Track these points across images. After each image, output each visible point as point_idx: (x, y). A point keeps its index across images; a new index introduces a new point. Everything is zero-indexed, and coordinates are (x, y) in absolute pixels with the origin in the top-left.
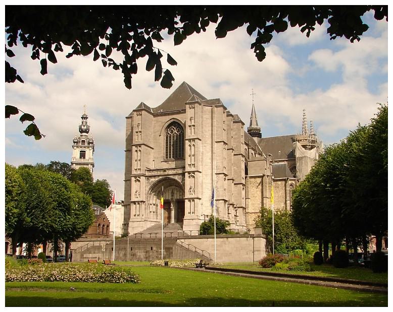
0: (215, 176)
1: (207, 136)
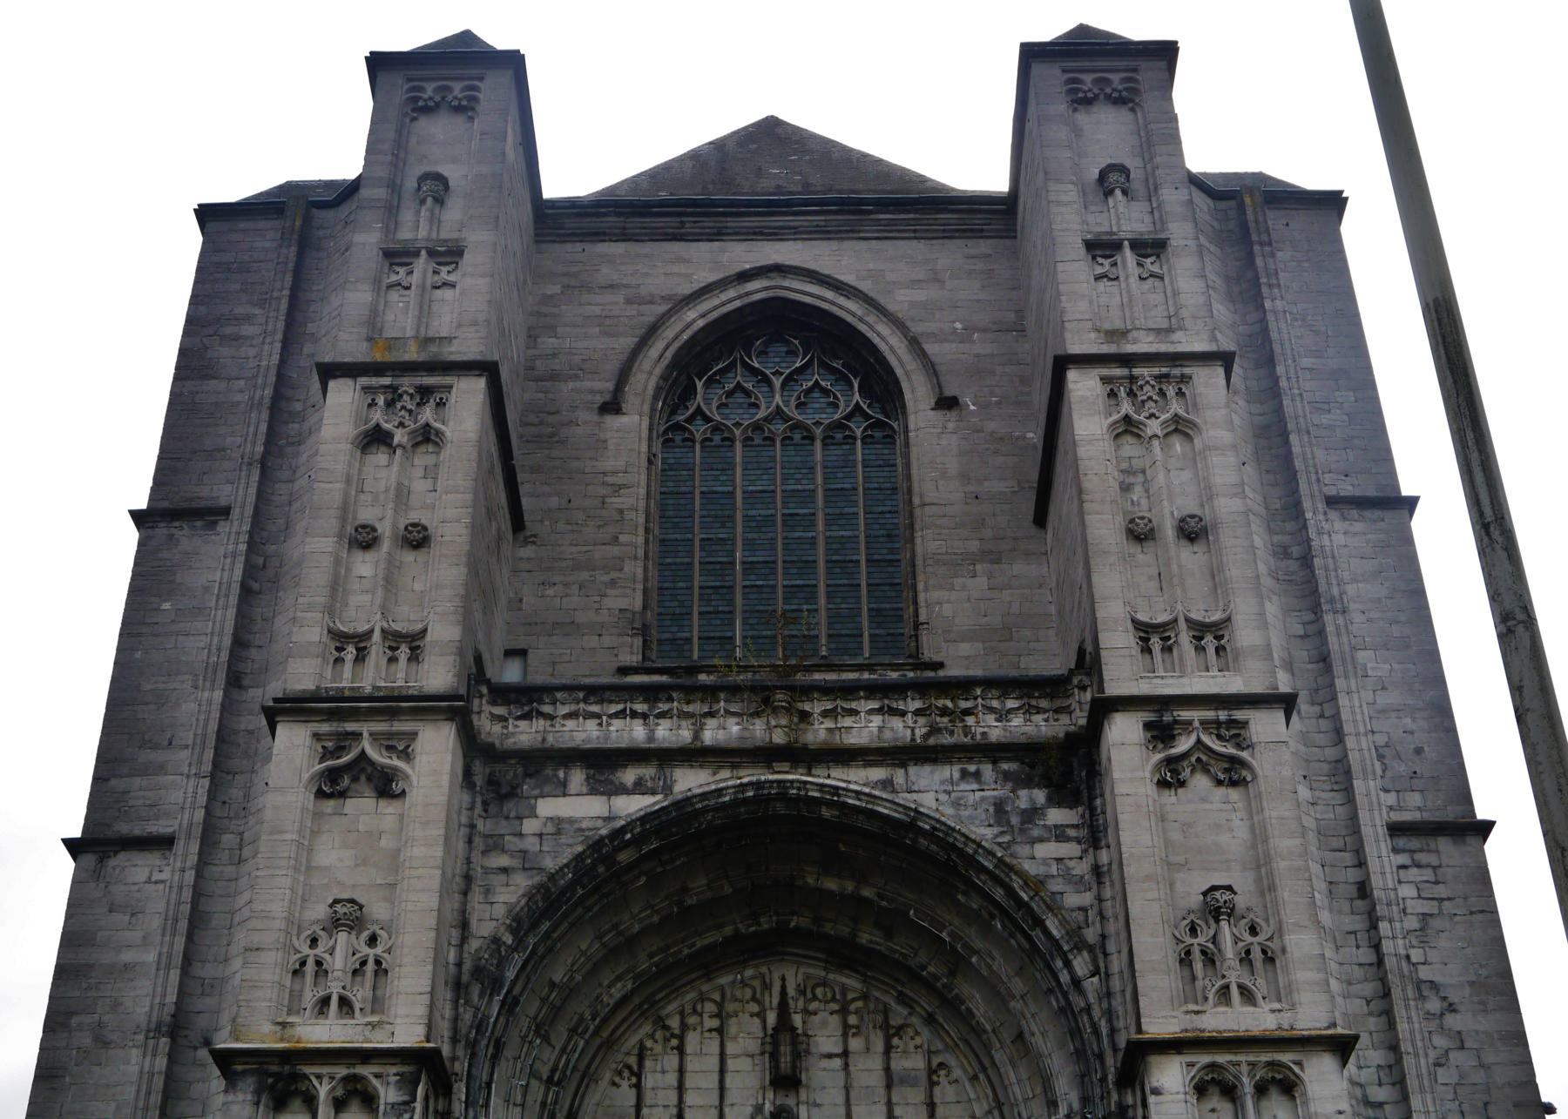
0: (1382, 857)
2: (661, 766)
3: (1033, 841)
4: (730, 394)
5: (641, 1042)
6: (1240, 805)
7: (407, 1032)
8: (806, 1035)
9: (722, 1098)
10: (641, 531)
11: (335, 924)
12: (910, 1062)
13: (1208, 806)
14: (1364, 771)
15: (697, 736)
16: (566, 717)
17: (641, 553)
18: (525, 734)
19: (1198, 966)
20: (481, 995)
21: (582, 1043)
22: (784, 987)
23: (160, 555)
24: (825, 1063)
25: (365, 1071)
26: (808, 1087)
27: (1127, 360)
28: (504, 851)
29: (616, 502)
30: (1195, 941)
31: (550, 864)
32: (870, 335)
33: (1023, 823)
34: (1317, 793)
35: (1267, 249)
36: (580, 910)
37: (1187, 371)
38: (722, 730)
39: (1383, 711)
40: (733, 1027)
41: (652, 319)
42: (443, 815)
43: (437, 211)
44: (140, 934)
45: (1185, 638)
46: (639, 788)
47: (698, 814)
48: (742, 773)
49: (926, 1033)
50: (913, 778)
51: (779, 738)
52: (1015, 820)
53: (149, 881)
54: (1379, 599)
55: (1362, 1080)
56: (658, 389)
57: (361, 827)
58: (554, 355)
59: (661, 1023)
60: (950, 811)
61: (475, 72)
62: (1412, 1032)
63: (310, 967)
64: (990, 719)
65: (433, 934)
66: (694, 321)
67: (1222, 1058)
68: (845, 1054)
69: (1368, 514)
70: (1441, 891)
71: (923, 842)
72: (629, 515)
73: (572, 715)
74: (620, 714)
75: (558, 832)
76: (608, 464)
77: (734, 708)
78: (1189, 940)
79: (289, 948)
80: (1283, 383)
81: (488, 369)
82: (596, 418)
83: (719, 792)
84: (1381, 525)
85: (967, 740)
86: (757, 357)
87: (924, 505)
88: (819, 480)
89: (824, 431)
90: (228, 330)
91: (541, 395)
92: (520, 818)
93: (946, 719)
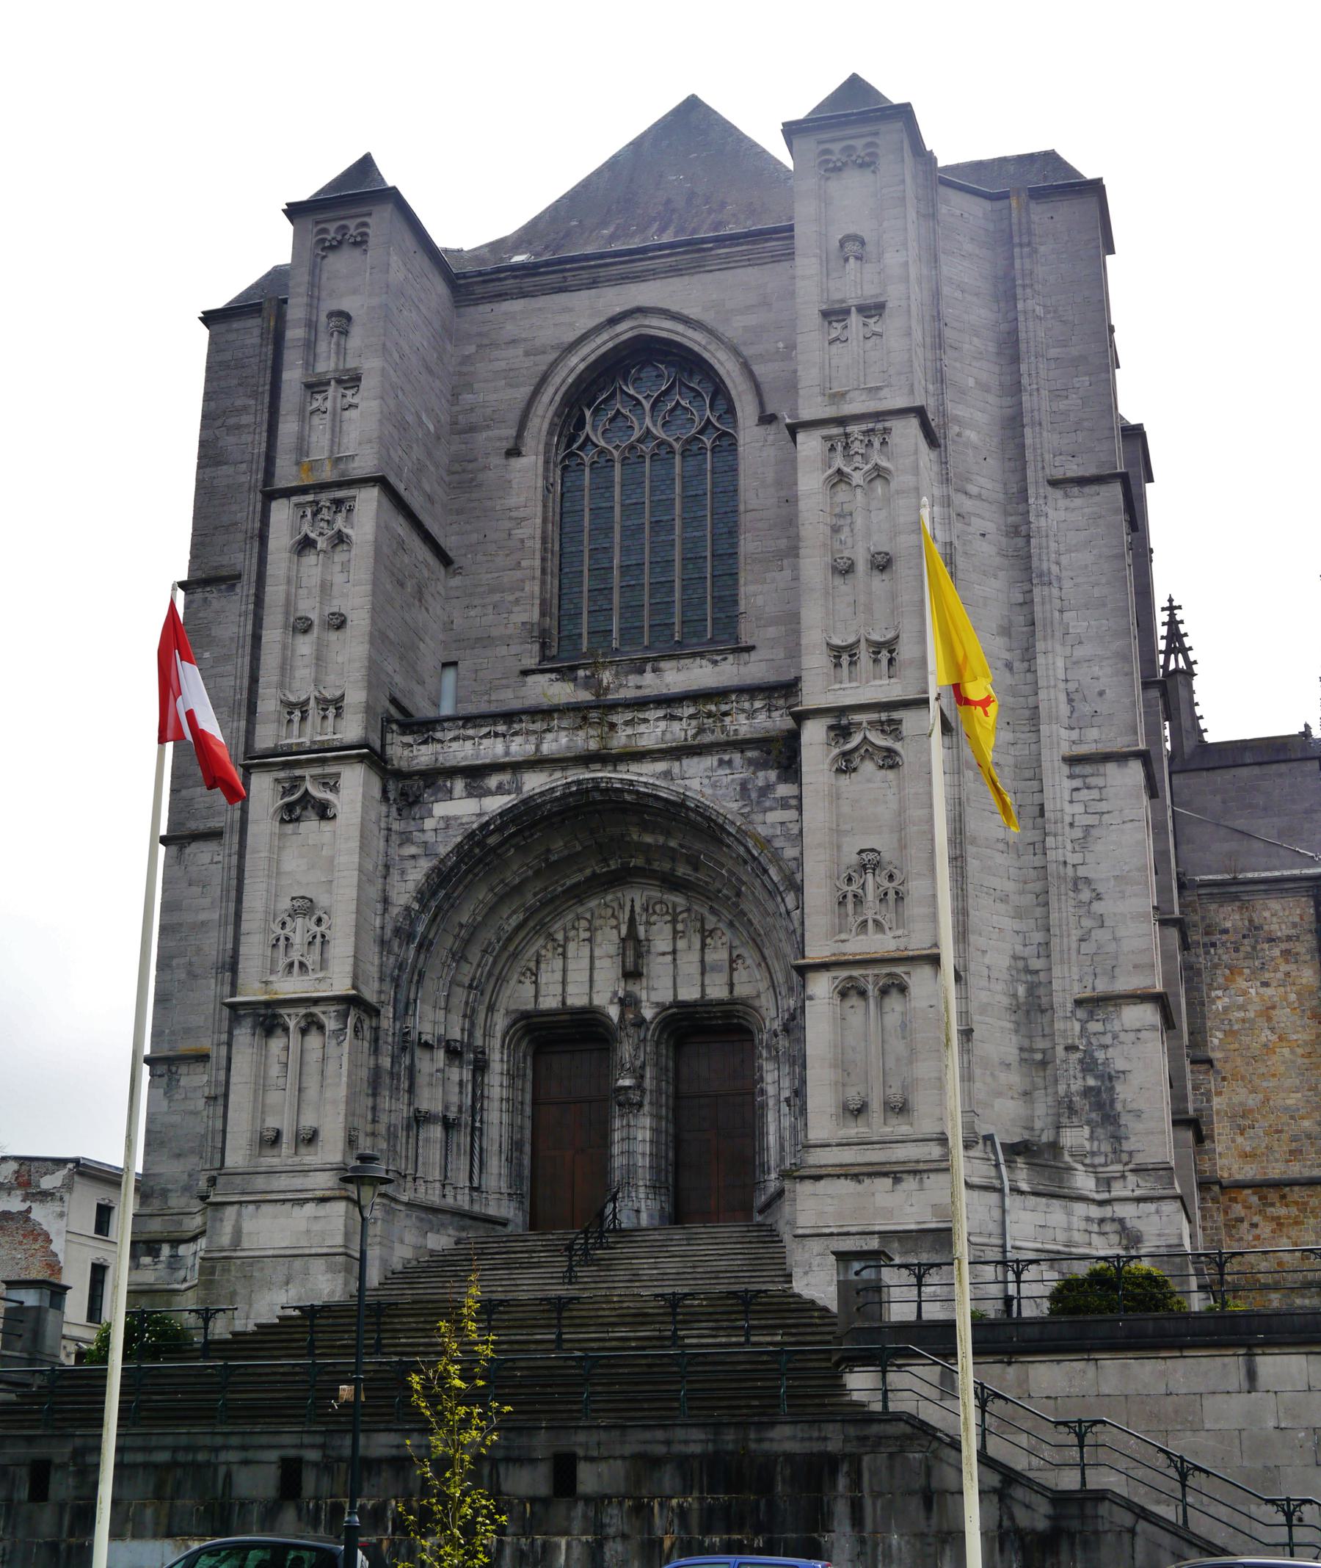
0: (1058, 784)
1: (972, 435)
2: (514, 773)
3: (765, 811)
4: (612, 420)
5: (537, 952)
6: (894, 783)
7: (340, 984)
8: (648, 940)
9: (591, 987)
10: (538, 556)
11: (293, 913)
12: (718, 955)
13: (871, 785)
14: (1050, 717)
15: (538, 749)
16: (450, 740)
17: (538, 573)
18: (424, 756)
19: (850, 906)
20: (400, 946)
21: (491, 959)
22: (632, 906)
23: (200, 615)
24: (661, 959)
25: (316, 1010)
26: (648, 977)
27: (841, 421)
28: (413, 843)
29: (518, 533)
30: (850, 888)
31: (443, 851)
32: (712, 361)
33: (759, 797)
34: (1018, 735)
35: (1026, 250)
36: (470, 876)
37: (887, 424)
38: (557, 742)
39: (1075, 663)
40: (599, 937)
41: (544, 368)
42: (358, 834)
43: (342, 342)
44: (209, 900)
45: (864, 654)
46: (500, 790)
47: (539, 806)
48: (569, 773)
49: (729, 934)
50: (685, 768)
51: (593, 745)
52: (754, 795)
53: (212, 863)
54: (1086, 566)
55: (1026, 955)
56: (552, 424)
57: (310, 842)
58: (472, 410)
59: (551, 937)
60: (708, 791)
61: (365, 209)
62: (1060, 919)
63: (282, 942)
64: (742, 718)
65: (354, 916)
66: (577, 365)
67: (856, 973)
68: (674, 952)
69: (1088, 490)
70: (1104, 806)
71: (692, 815)
72: (528, 543)
73: (455, 739)
74: (487, 735)
75: (447, 827)
76: (512, 501)
77: (565, 724)
78: (846, 888)
79: (267, 930)
80: (1025, 381)
81: (381, 482)
82: (503, 461)
83: (552, 790)
84: (1097, 499)
85: (723, 737)
86: (633, 384)
87: (746, 511)
88: (678, 489)
89: (683, 445)
90: (232, 421)
91: (463, 446)
92: (422, 819)
93: (711, 720)
